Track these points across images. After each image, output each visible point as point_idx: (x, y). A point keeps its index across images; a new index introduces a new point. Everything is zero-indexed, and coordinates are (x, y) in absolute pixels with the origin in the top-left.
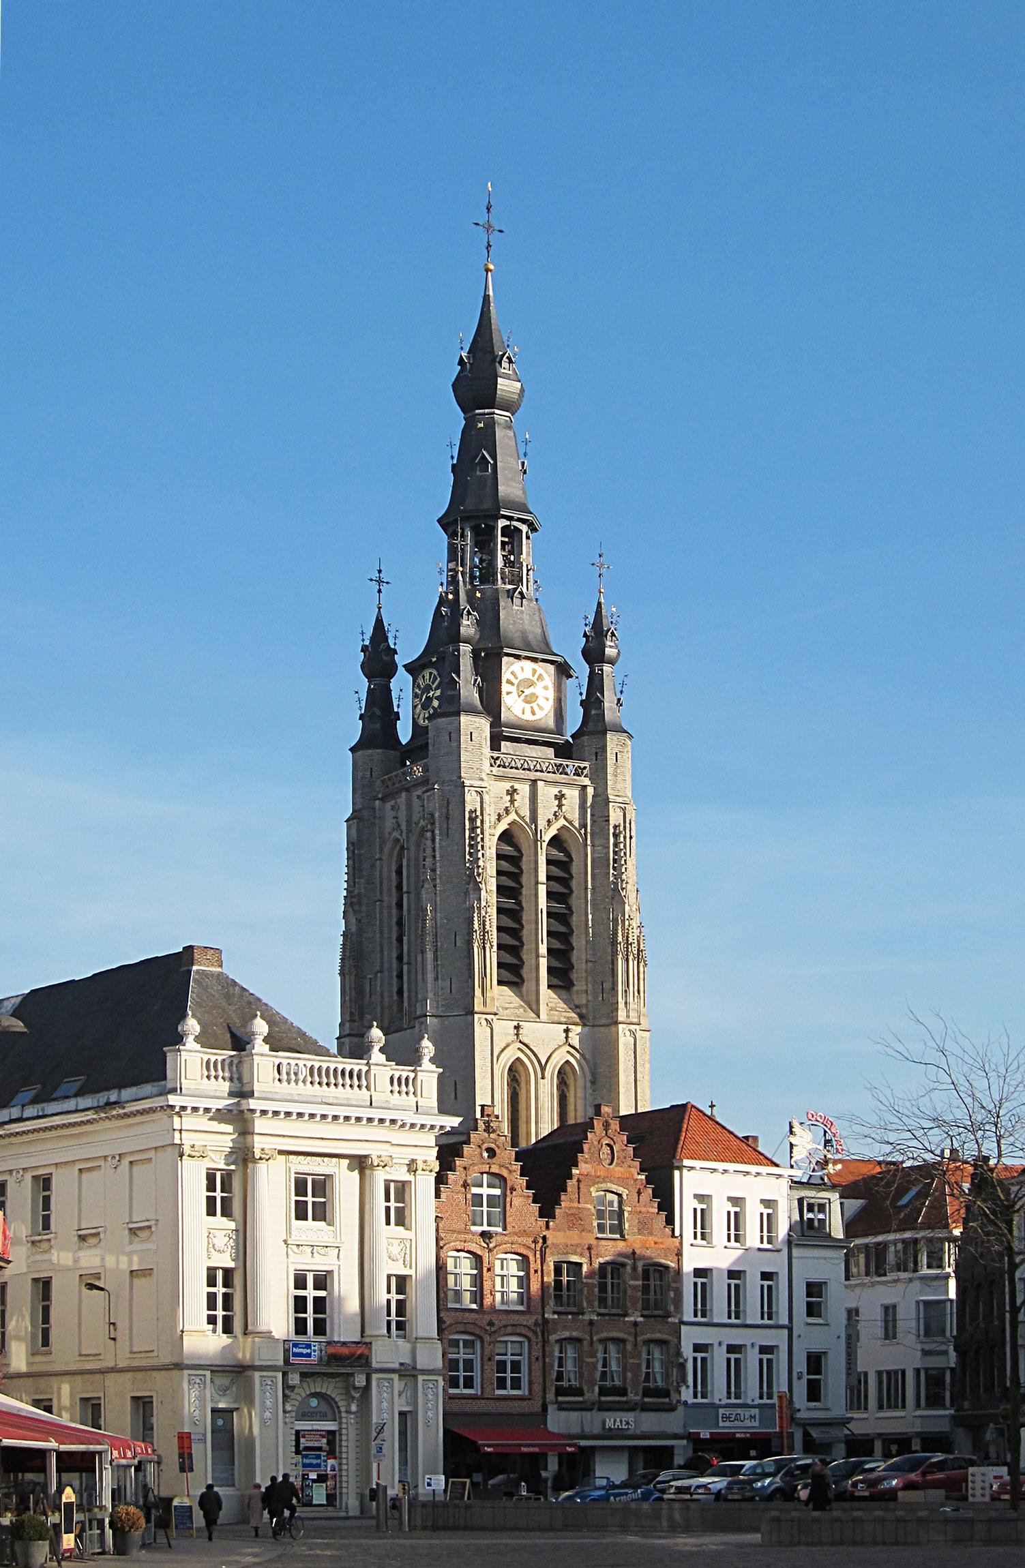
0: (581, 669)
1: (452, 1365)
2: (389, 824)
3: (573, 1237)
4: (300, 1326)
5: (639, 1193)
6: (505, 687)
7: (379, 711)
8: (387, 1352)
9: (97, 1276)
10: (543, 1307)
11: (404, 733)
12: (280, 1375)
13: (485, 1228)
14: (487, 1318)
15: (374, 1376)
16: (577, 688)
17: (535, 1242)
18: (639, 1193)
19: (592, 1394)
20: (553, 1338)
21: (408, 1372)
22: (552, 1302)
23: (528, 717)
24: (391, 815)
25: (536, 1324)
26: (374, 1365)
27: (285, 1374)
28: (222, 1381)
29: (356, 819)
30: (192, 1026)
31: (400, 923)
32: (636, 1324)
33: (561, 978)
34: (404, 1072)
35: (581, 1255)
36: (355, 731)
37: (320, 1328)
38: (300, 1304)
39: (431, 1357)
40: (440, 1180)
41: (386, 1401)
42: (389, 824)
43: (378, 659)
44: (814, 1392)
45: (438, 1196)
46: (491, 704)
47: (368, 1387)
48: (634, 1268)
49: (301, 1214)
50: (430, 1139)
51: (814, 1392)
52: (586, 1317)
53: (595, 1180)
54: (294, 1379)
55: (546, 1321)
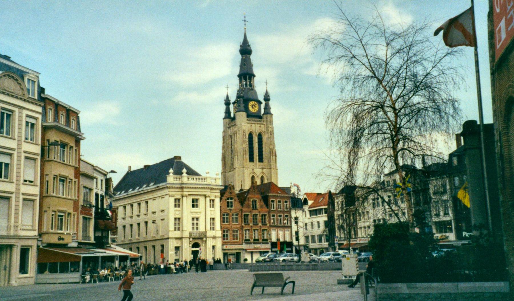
0: (264, 103)
1: (224, 235)
2: (230, 132)
3: (247, 210)
4: (193, 228)
6: (249, 106)
7: (228, 112)
8: (210, 233)
9: (155, 221)
11: (232, 115)
13: (230, 208)
15: (207, 239)
16: (263, 106)
19: (252, 241)
21: (214, 238)
24: (230, 132)
26: (208, 236)
27: (189, 239)
28: (177, 241)
29: (224, 132)
30: (171, 171)
31: (232, 151)
33: (261, 160)
36: (223, 115)
37: (197, 228)
38: (193, 224)
39: (219, 234)
40: (221, 199)
41: (210, 243)
42: (230, 132)
43: (227, 103)
44: (297, 239)
45: (220, 201)
46: (246, 110)
47: (206, 241)
49: (193, 206)
50: (219, 191)
51: (297, 239)
53: (251, 198)
54: (191, 239)
55: (242, 226)
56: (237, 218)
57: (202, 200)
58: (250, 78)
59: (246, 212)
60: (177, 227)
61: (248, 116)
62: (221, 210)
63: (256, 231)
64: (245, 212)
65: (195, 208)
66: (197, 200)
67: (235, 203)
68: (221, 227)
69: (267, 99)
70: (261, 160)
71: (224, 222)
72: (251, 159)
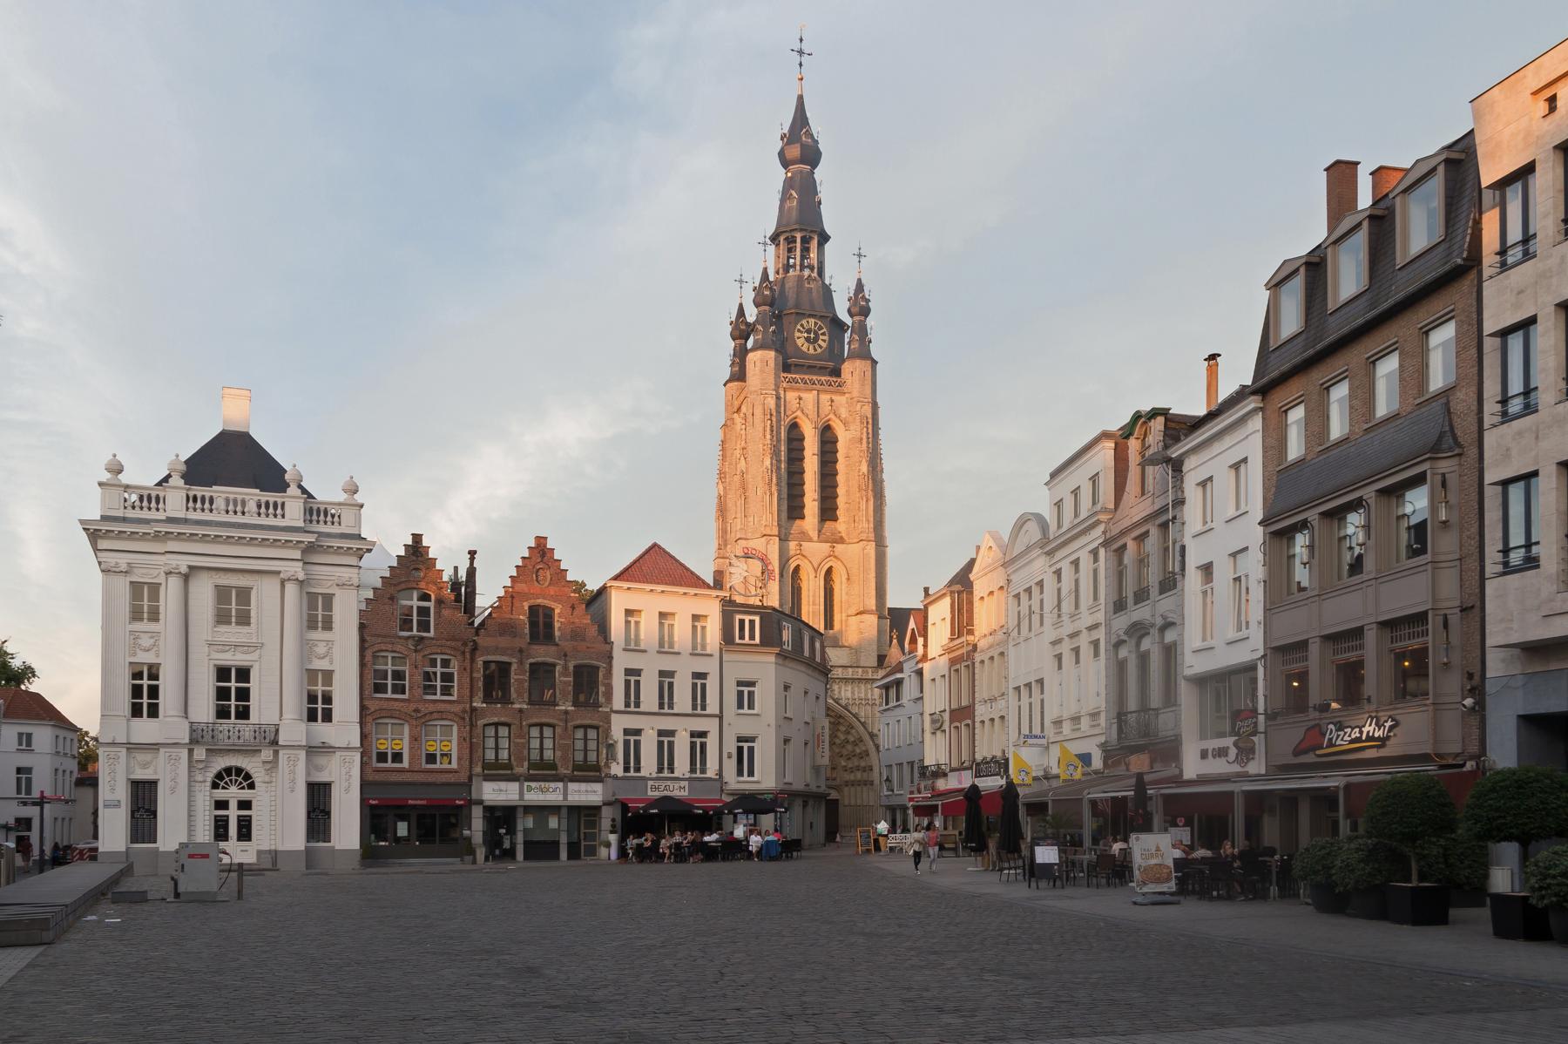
3: (504, 641)
5: (573, 608)
10: (471, 697)
12: (185, 753)
14: (413, 706)
17: (465, 644)
18: (573, 608)
19: (521, 769)
20: (481, 723)
22: (481, 694)
23: (812, 351)
25: (464, 711)
27: (191, 751)
32: (566, 712)
33: (828, 511)
34: (271, 497)
35: (511, 655)
48: (565, 668)
52: (517, 706)
54: (200, 753)
55: (473, 710)
56: (447, 677)
57: (265, 595)
58: (806, 241)
59: (497, 650)
60: (145, 701)
61: (786, 368)
62: (362, 641)
63: (503, 731)
64: (487, 651)
65: (233, 628)
66: (244, 595)
67: (438, 613)
68: (363, 708)
69: (861, 308)
70: (828, 511)
71: (379, 688)
72: (794, 509)
